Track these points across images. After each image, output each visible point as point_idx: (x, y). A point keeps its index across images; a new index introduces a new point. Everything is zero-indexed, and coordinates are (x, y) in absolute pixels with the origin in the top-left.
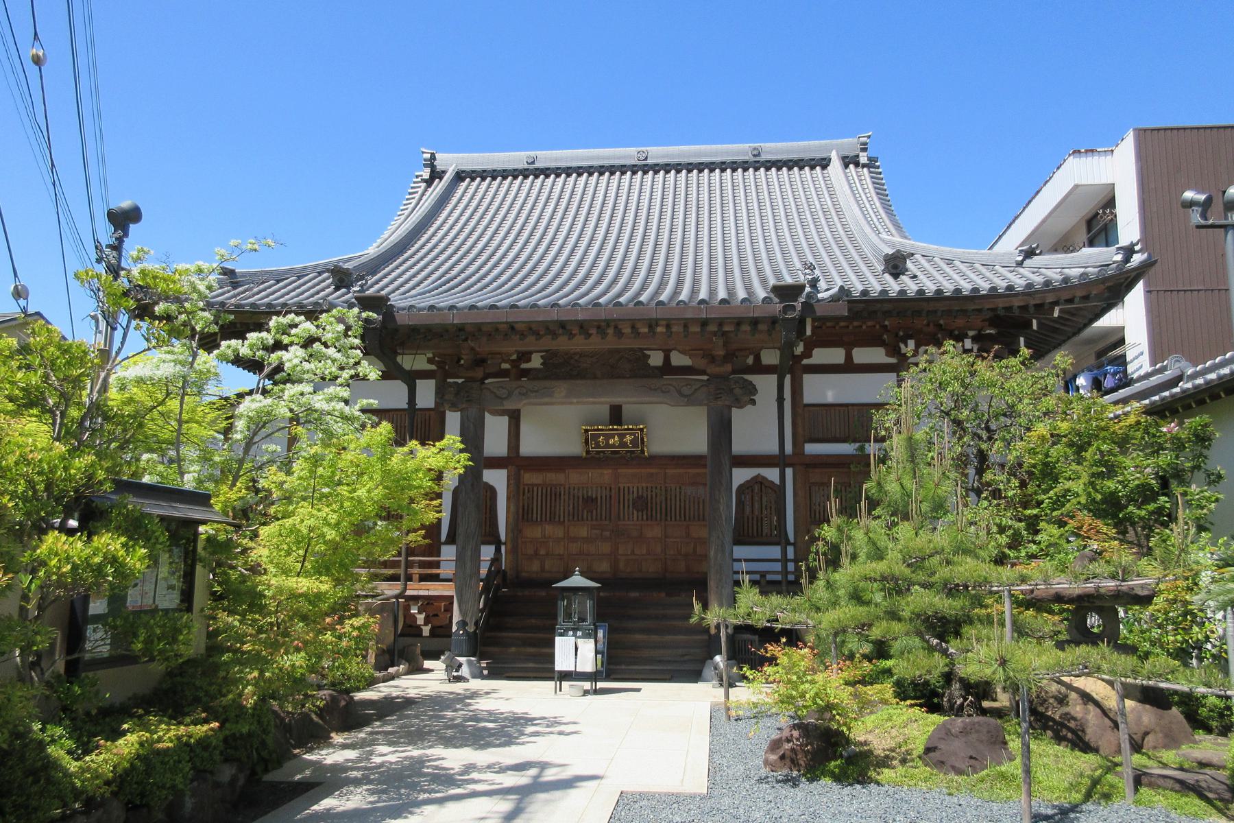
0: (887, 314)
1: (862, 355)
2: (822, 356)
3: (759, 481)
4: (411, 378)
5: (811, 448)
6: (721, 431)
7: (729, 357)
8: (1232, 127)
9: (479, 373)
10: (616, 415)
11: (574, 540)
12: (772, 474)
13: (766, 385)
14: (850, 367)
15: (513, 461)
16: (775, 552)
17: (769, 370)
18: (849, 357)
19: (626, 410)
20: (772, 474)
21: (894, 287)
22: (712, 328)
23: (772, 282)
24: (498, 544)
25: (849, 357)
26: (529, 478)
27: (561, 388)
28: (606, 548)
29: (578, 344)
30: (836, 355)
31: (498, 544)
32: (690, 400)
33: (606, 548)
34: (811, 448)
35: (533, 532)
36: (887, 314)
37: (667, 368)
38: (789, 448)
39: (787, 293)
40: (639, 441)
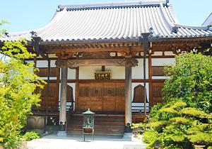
0: (173, 42)
1: (167, 53)
2: (156, 54)
3: (140, 86)
4: (49, 60)
5: (153, 78)
6: (128, 73)
7: (131, 53)
8: (204, 45)
9: (66, 58)
10: (103, 67)
11: (92, 101)
12: (143, 84)
13: (141, 61)
14: (163, 56)
15: (77, 81)
16: (143, 104)
17: (142, 57)
18: (163, 54)
19: (106, 67)
20: (143, 84)
21: (174, 35)
22: (126, 45)
23: (143, 32)
24: (73, 102)
25: (163, 54)
26: (81, 85)
27: (87, 62)
28: (101, 103)
29: (91, 50)
30: (160, 53)
31: (73, 102)
32: (121, 65)
33: (101, 103)
34: (153, 78)
35: (81, 99)
36: (173, 42)
37: (116, 57)
38: (147, 78)
39: (145, 35)
40: (109, 76)
